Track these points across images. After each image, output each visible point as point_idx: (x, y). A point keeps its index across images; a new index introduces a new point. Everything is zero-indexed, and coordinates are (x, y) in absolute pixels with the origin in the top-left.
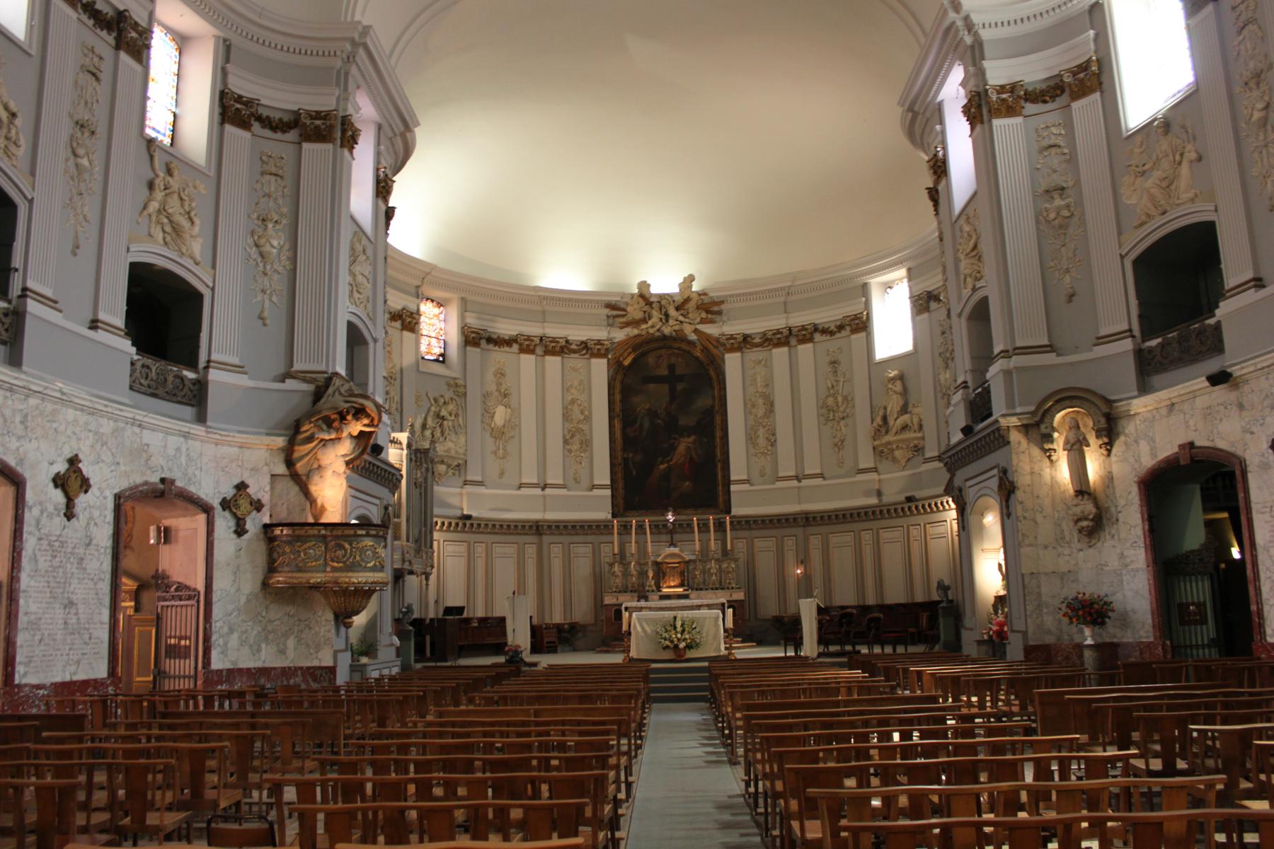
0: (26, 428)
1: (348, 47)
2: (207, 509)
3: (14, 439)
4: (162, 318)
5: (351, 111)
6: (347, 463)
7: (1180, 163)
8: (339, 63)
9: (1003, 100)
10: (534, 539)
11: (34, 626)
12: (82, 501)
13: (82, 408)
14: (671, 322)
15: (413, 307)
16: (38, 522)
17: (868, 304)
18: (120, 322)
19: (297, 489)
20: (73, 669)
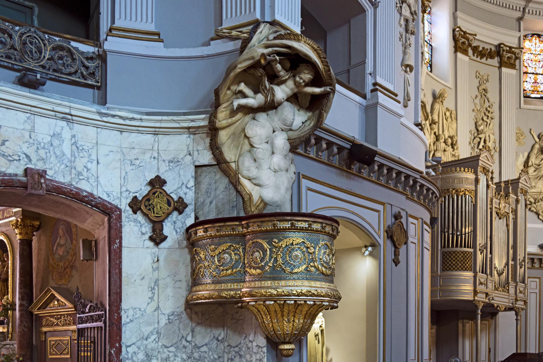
2: (109, 211)
19: (226, 181)
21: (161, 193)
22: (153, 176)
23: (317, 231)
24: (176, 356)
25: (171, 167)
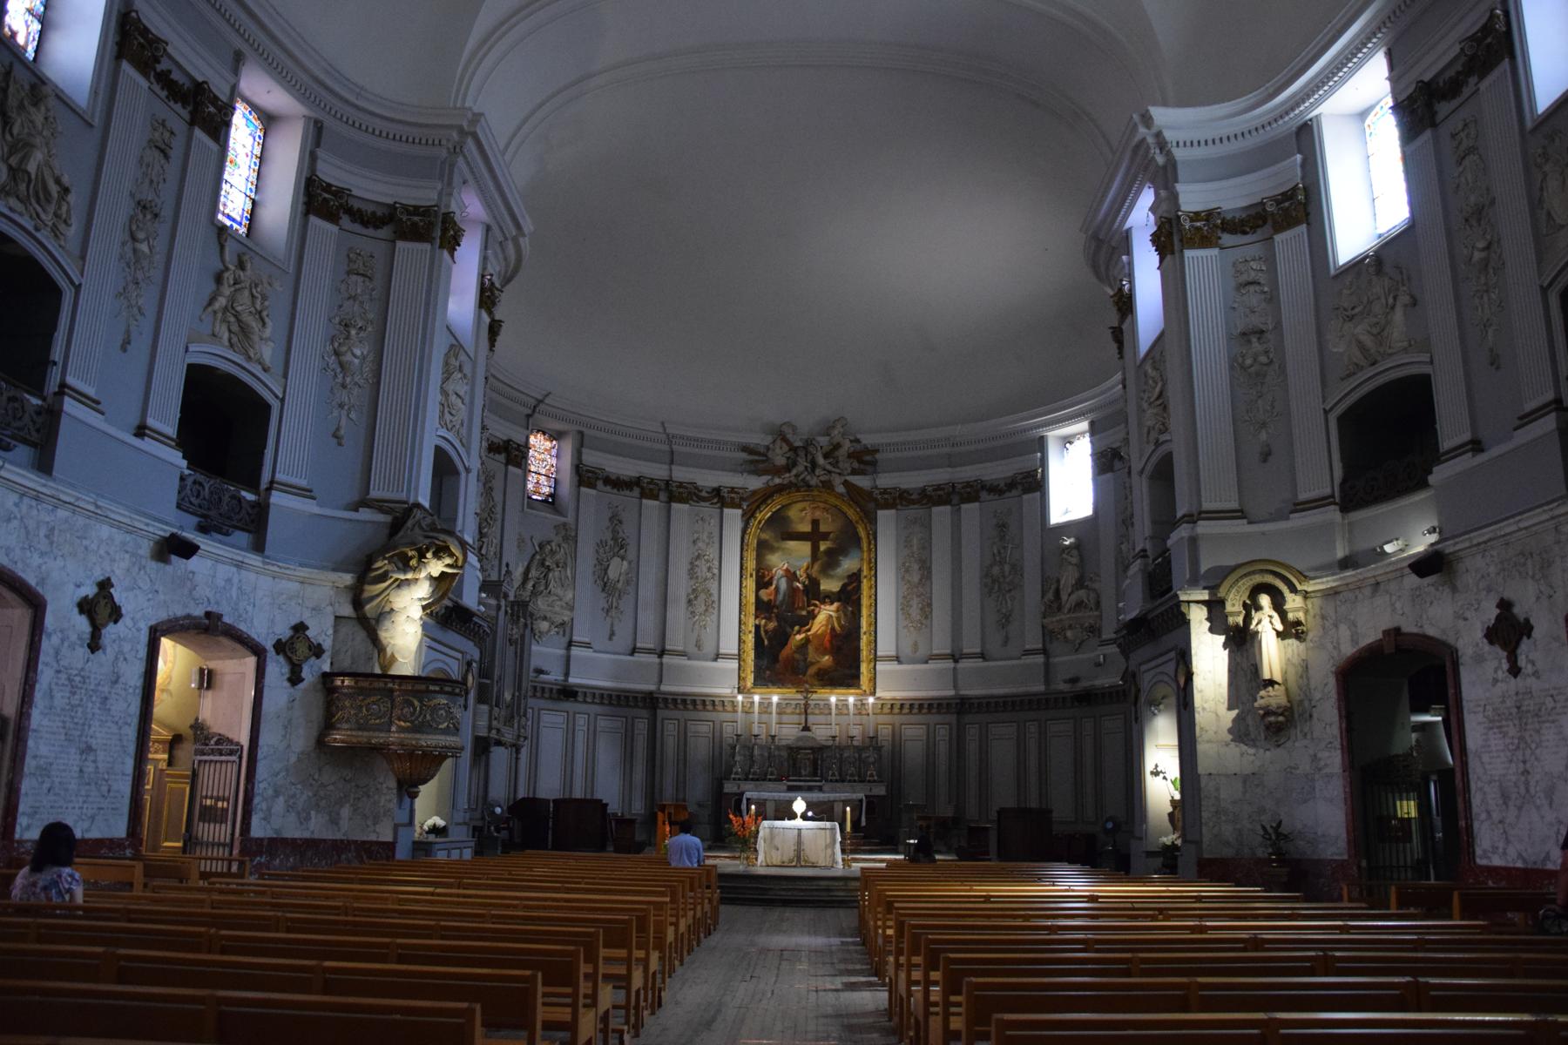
0: (52, 543)
1: (455, 135)
2: (258, 651)
3: (36, 556)
4: (222, 430)
5: (453, 207)
6: (424, 608)
7: (1393, 308)
8: (444, 153)
9: (1198, 229)
10: (645, 713)
11: (45, 771)
12: (110, 631)
13: (118, 525)
14: (818, 472)
15: (518, 438)
16: (57, 653)
17: (1044, 463)
18: (171, 430)
20: (86, 825)
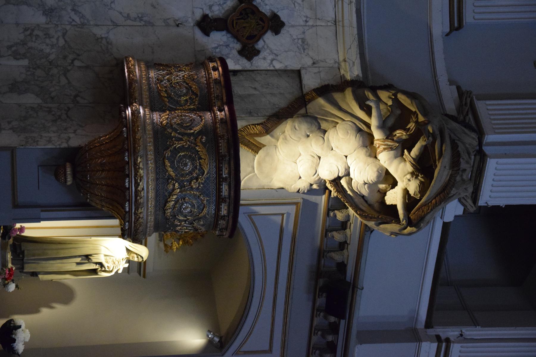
21: (263, 28)
22: (283, 17)
23: (219, 190)
24: (53, 46)
25: (296, 41)
